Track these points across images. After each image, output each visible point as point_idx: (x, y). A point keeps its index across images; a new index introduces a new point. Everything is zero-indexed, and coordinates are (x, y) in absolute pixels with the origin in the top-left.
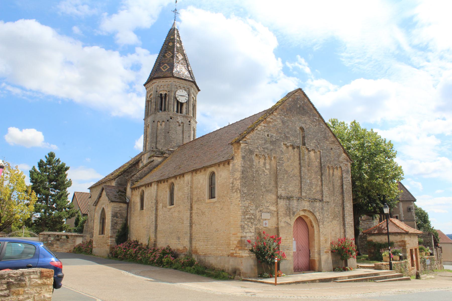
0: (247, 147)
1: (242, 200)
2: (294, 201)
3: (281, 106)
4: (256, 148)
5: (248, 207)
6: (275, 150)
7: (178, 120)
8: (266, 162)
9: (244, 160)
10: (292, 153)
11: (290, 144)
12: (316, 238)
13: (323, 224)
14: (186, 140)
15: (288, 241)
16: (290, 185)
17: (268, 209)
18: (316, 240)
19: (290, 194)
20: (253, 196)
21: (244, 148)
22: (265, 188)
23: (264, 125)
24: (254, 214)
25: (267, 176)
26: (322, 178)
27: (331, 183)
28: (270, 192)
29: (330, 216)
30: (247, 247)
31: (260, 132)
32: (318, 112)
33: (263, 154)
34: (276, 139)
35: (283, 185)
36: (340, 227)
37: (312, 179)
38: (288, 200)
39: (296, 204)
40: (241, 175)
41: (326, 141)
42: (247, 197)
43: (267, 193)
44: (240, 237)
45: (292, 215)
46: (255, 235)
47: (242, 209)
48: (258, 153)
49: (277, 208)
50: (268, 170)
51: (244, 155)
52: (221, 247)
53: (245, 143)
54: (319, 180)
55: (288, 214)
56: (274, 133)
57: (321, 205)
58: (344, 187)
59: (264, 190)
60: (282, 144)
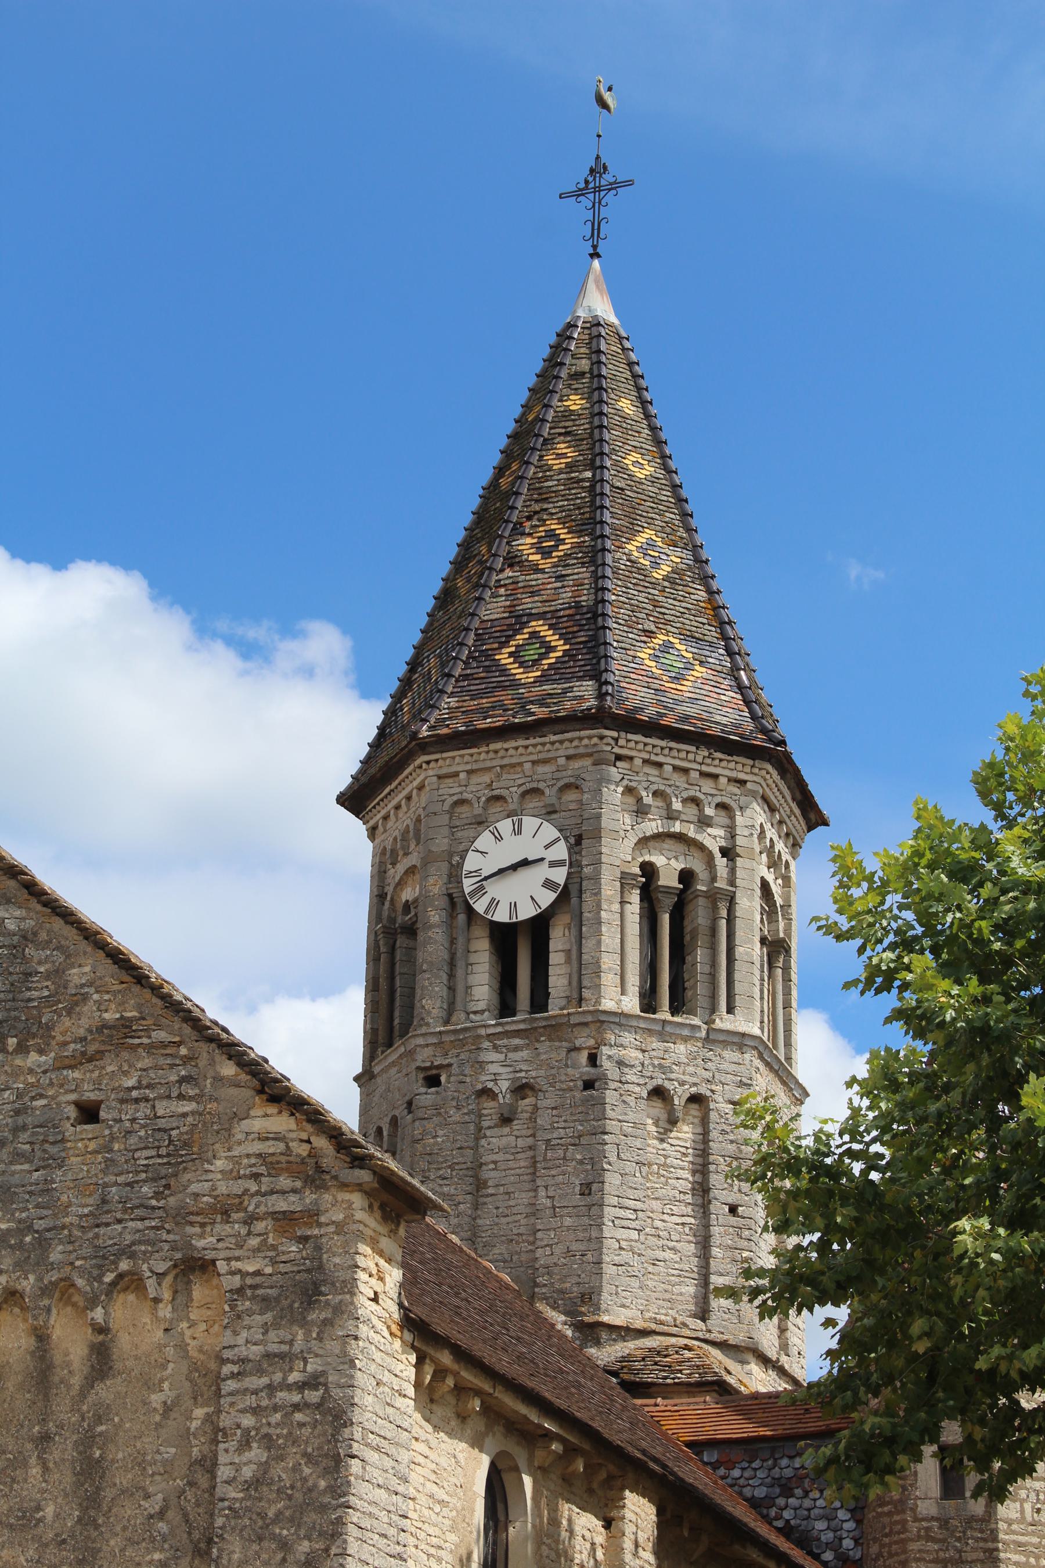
7: (484, 1080)
14: (554, 1222)
27: (64, 1449)
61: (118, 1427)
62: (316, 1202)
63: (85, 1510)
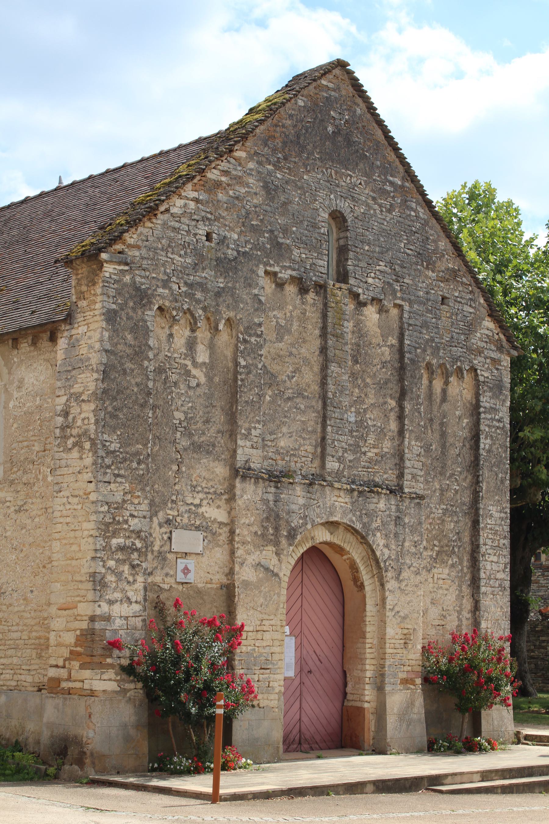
0: (127, 279)
1: (100, 478)
2: (294, 489)
3: (262, 127)
4: (159, 284)
5: (120, 506)
6: (232, 296)
8: (196, 338)
9: (113, 326)
10: (295, 307)
11: (289, 272)
12: (370, 629)
13: (397, 578)
15: (267, 636)
16: (285, 429)
17: (196, 514)
18: (368, 635)
19: (280, 462)
20: (143, 466)
21: (116, 282)
22: (190, 435)
23: (195, 194)
24: (143, 534)
25: (199, 391)
26: (401, 408)
27: (436, 426)
28: (208, 453)
29: (425, 548)
30: (111, 656)
31: (179, 222)
32: (402, 158)
33: (186, 307)
34: (238, 252)
35: (255, 428)
36: (461, 591)
37: (365, 410)
38: (272, 484)
39: (301, 501)
40: (100, 385)
41: (427, 268)
42: (119, 469)
43: (195, 455)
44: (87, 618)
45: (284, 541)
46: (145, 610)
47: (96, 512)
48: (167, 304)
49: (229, 513)
50: (204, 370)
51: (114, 306)
52: (11, 657)
53: (120, 263)
54: (393, 416)
55: (272, 537)
56: (232, 229)
57: (393, 508)
58: (482, 446)
59: (185, 443)
60: (261, 272)
61: (449, 421)
62: (500, 357)
63: (442, 449)
